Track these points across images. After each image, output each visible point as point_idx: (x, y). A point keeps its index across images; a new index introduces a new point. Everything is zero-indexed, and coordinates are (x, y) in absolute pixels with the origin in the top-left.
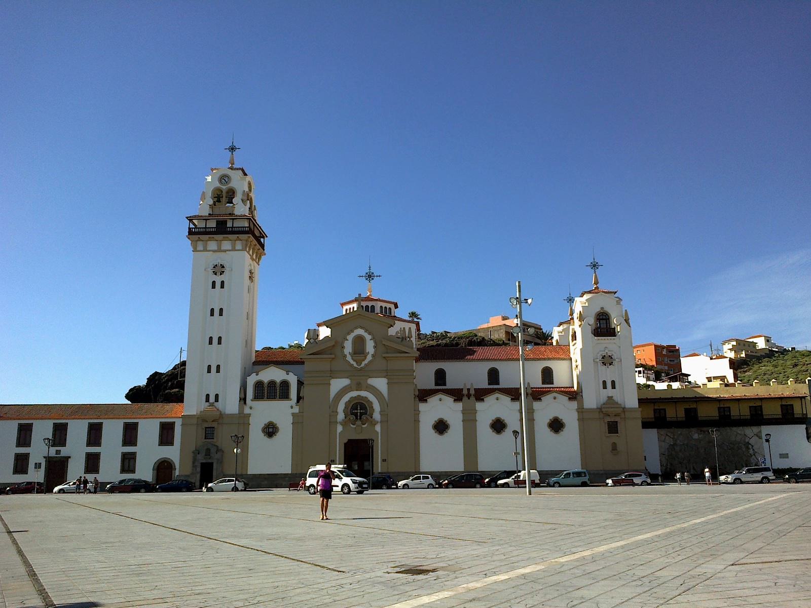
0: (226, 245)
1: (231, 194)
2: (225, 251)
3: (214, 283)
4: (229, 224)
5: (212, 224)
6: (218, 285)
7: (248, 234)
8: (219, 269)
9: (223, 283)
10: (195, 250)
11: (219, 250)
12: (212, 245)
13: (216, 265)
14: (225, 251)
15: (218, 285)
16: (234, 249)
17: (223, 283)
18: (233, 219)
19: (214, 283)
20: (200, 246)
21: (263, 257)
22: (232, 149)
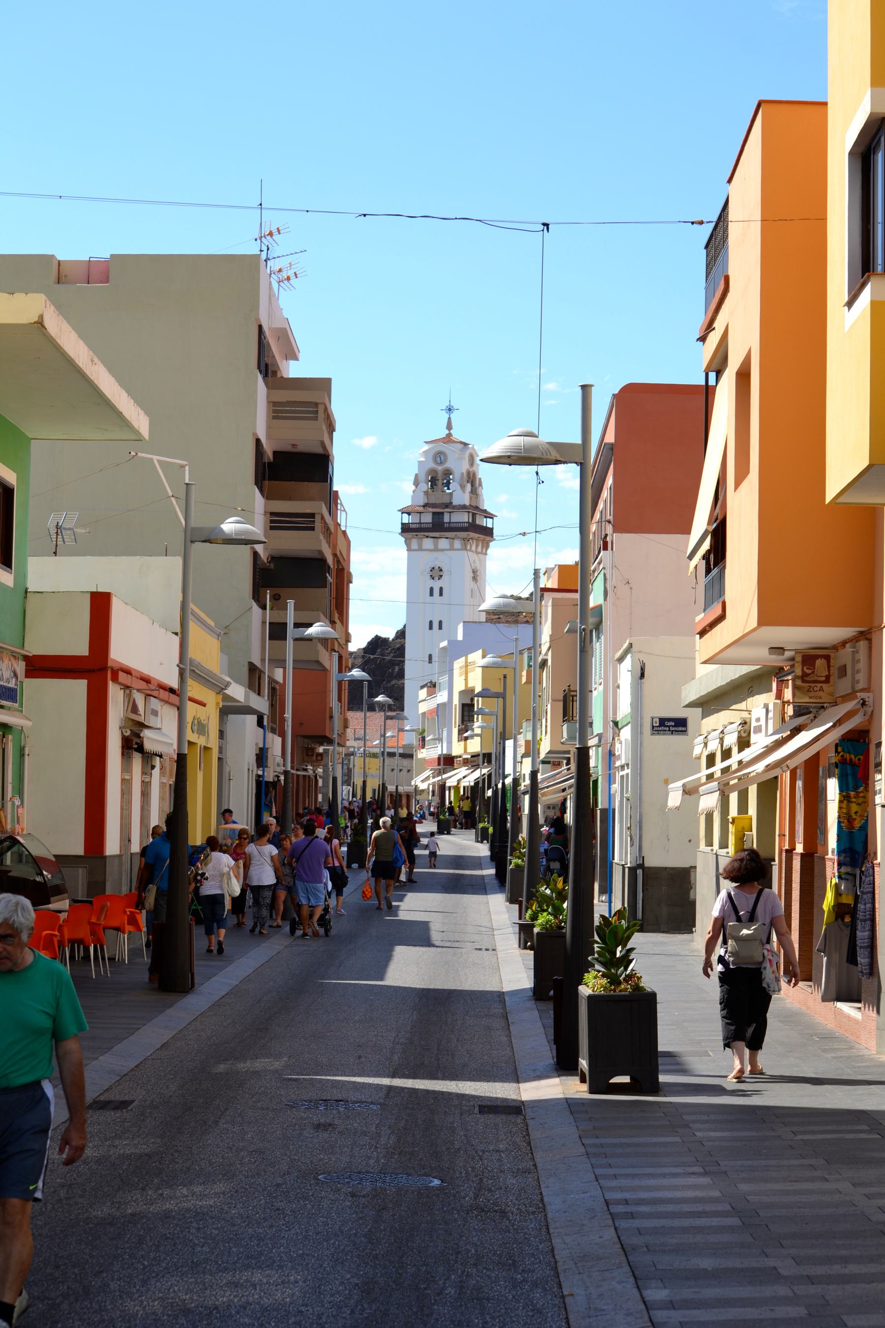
0: (443, 543)
1: (448, 473)
2: (443, 550)
3: (432, 589)
4: (446, 519)
5: (427, 518)
6: (436, 592)
7: (468, 531)
8: (436, 573)
9: (441, 589)
10: (409, 549)
11: (436, 549)
12: (428, 543)
13: (433, 568)
14: (443, 550)
15: (436, 592)
16: (452, 549)
17: (441, 589)
18: (450, 512)
19: (432, 589)
20: (414, 544)
21: (491, 544)
22: (450, 410)
